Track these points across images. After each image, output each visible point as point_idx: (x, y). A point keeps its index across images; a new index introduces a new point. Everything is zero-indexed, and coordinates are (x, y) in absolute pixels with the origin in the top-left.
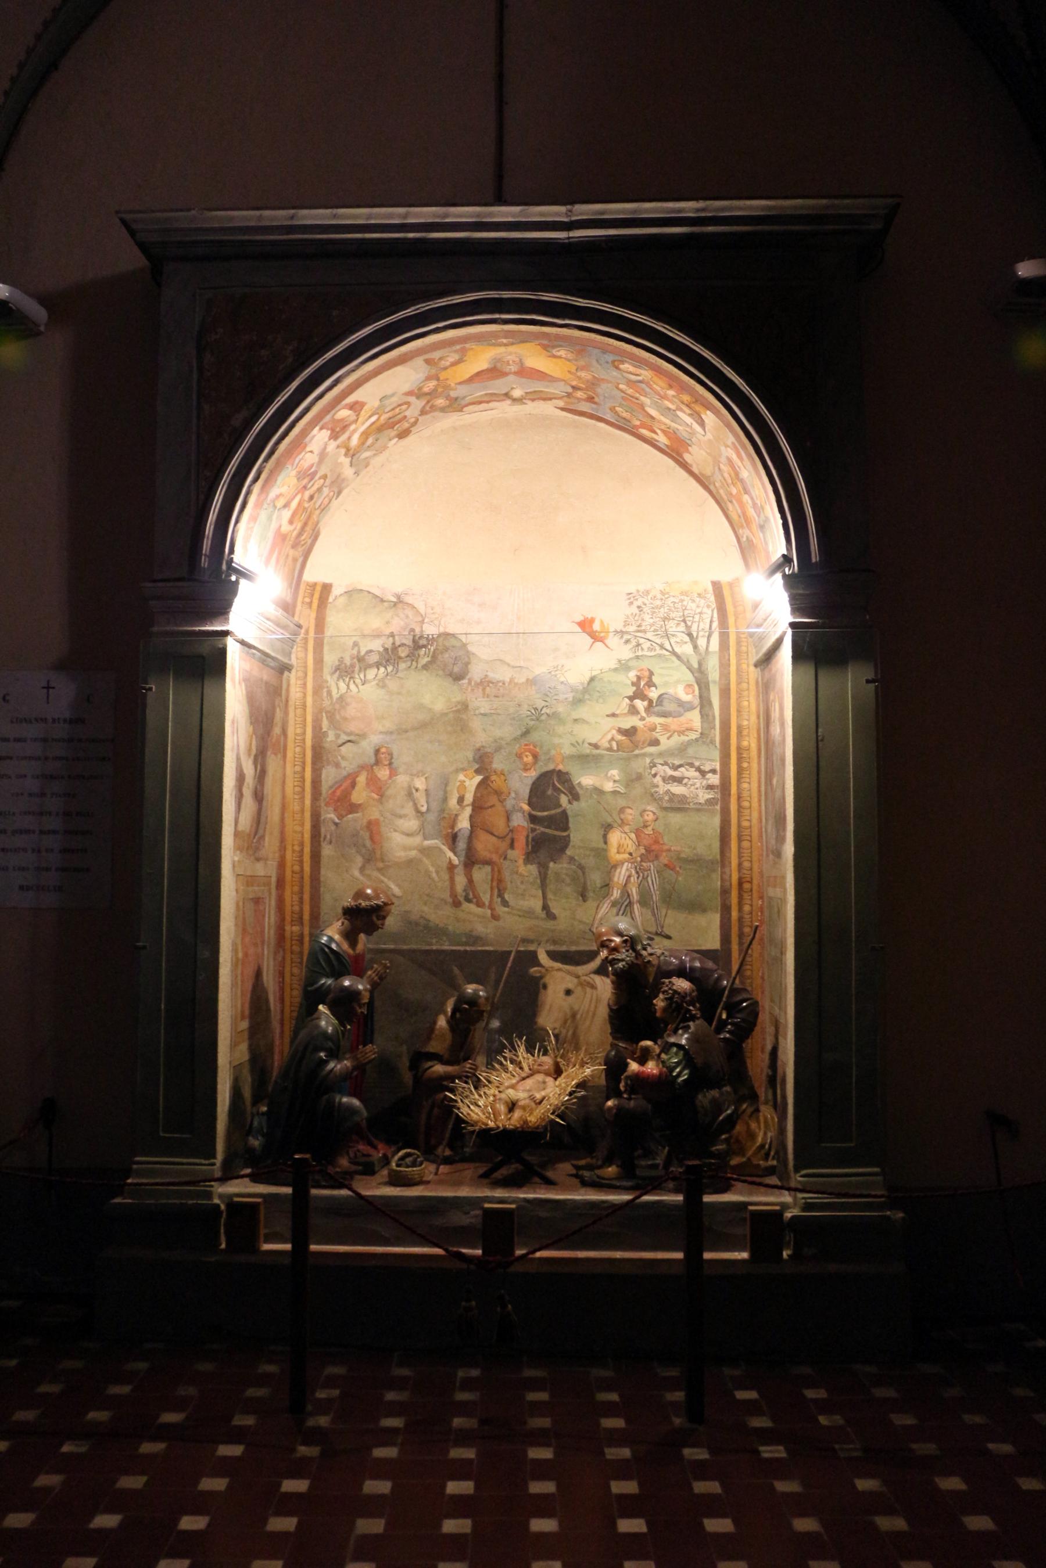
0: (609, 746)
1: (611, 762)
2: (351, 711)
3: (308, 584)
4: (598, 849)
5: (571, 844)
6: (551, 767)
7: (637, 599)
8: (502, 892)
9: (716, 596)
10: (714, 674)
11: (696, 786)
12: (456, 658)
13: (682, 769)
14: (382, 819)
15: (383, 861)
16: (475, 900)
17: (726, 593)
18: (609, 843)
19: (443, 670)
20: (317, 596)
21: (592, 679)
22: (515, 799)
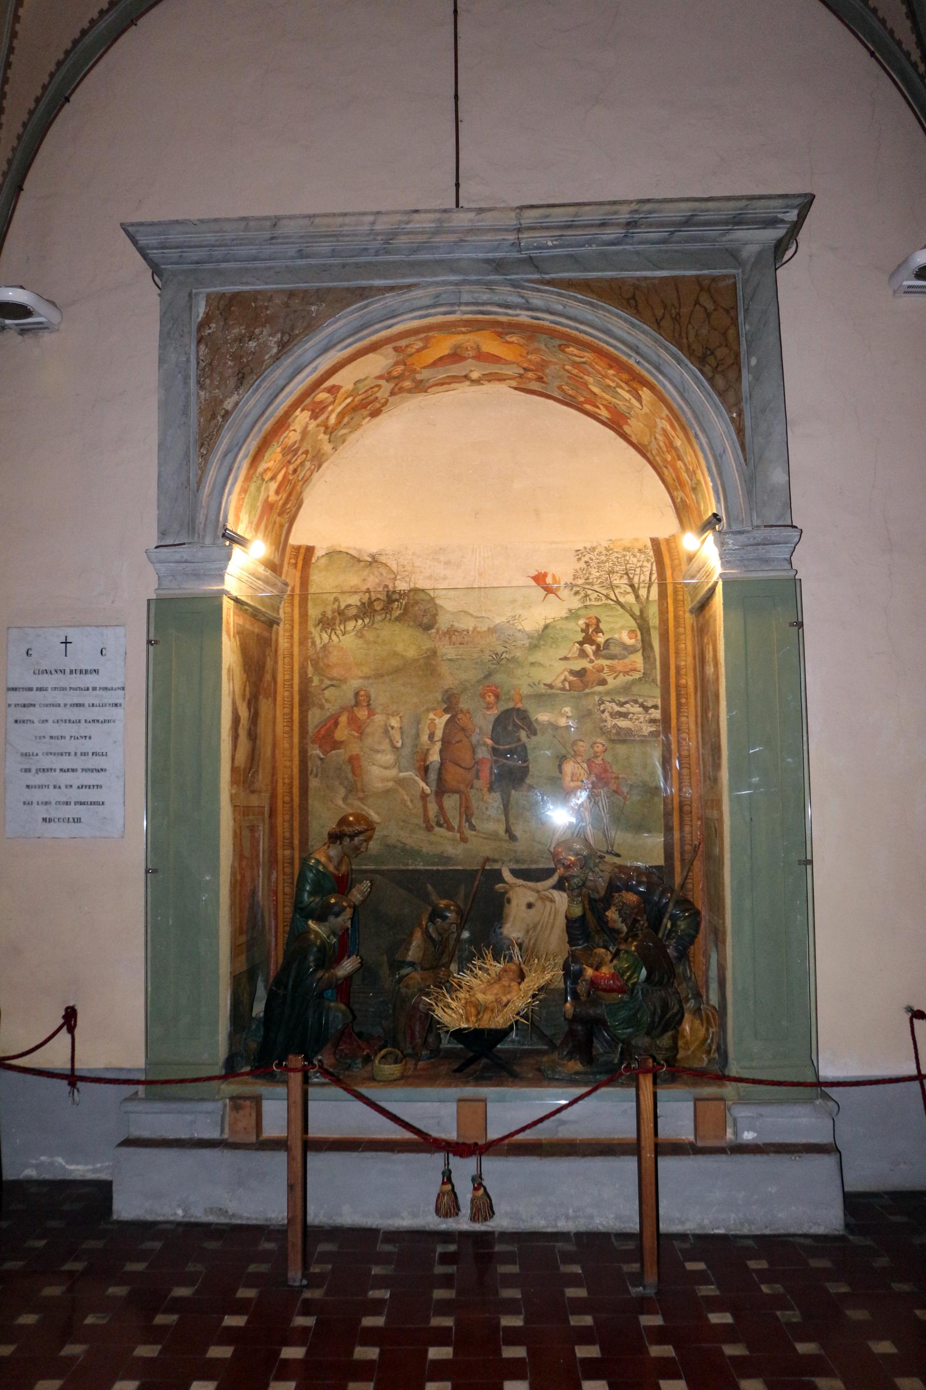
2: (334, 658)
3: (293, 547)
5: (530, 774)
6: (511, 705)
7: (584, 556)
9: (654, 551)
10: (654, 620)
12: (425, 610)
13: (628, 706)
14: (362, 754)
15: (363, 791)
16: (445, 825)
17: (664, 548)
18: (563, 772)
19: (414, 621)
20: (301, 557)
21: (546, 627)
22: (479, 734)
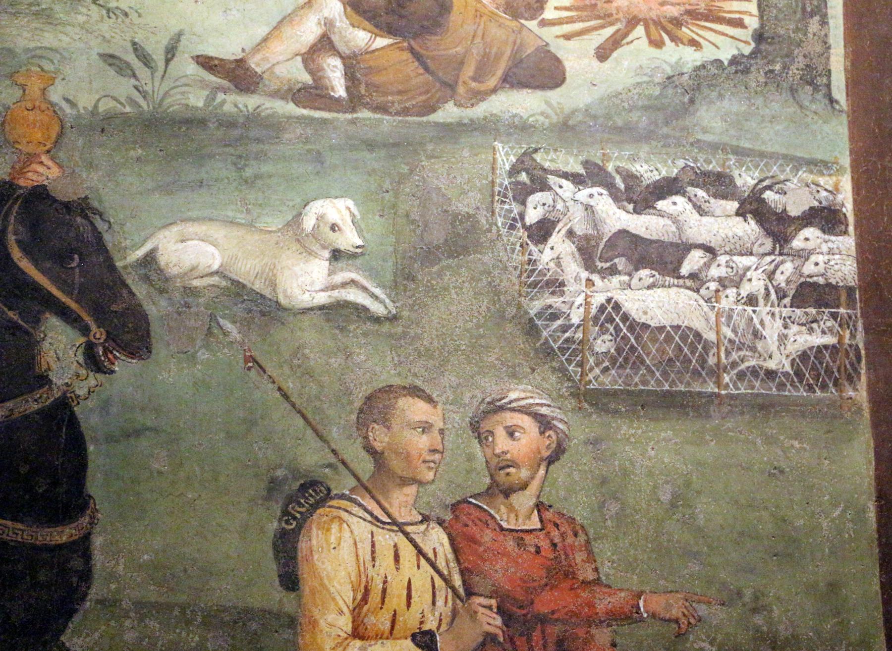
0: (306, 78)
1: (319, 158)
4: (247, 613)
5: (96, 591)
11: (746, 289)
18: (308, 583)
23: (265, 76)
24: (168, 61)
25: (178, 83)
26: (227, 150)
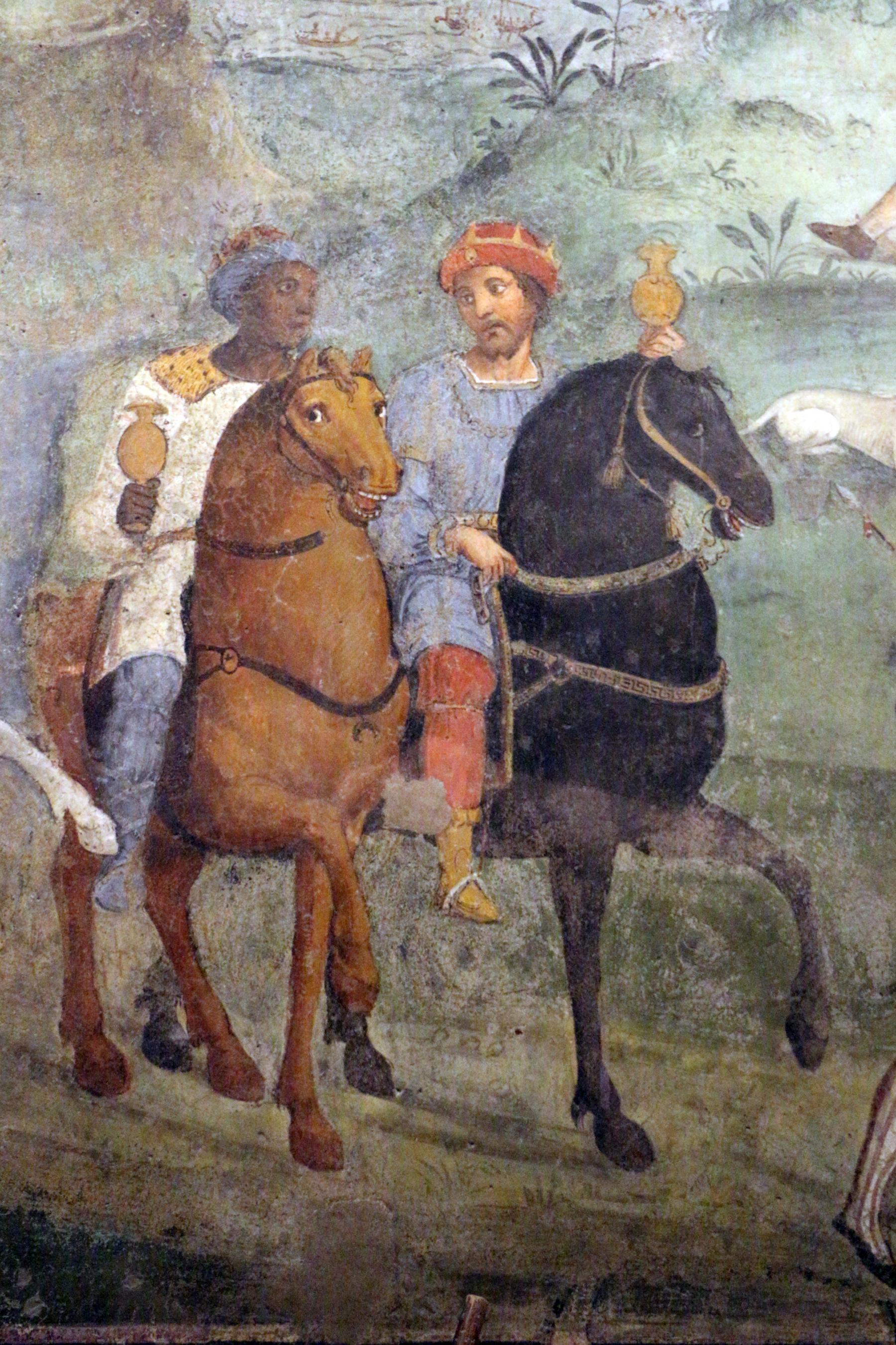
5: (730, 748)
8: (354, 1007)
16: (201, 1054)
22: (428, 505)
23: (879, 242)
24: (784, 230)
25: (794, 252)
26: (840, 317)
